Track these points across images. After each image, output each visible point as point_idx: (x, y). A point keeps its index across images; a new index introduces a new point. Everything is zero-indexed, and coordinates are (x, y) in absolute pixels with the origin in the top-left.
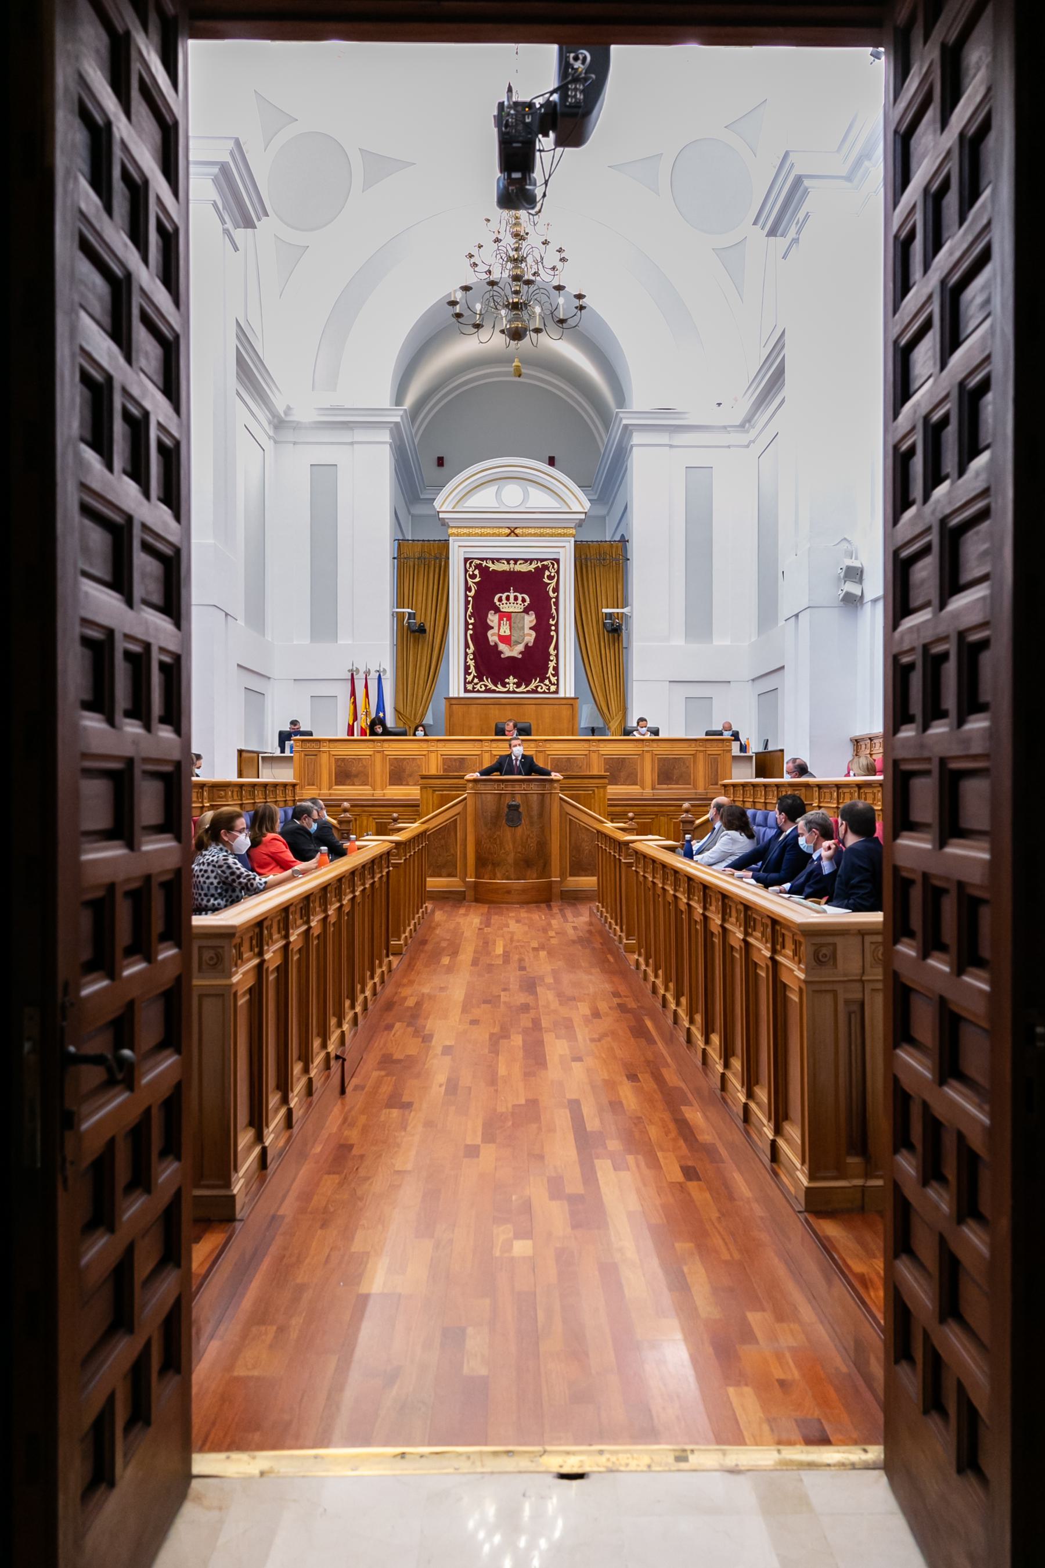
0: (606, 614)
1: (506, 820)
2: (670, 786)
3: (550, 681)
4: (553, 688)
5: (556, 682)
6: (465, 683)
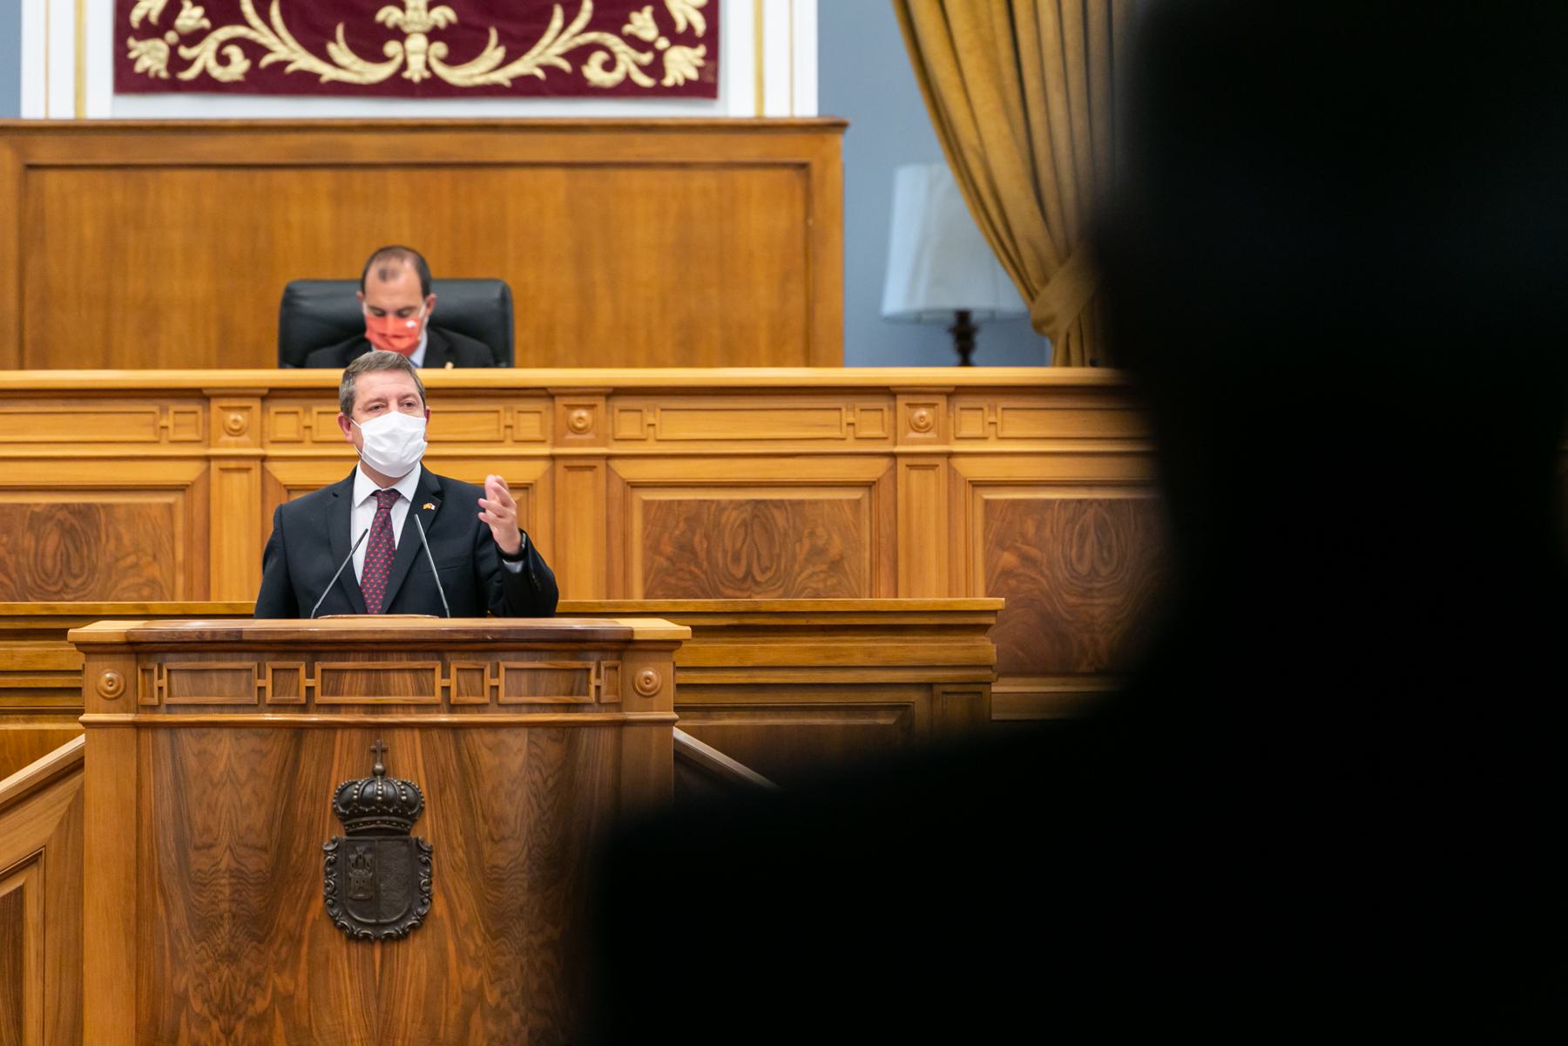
1: (336, 898)
4: (682, 64)
5: (700, 26)
6: (123, 31)
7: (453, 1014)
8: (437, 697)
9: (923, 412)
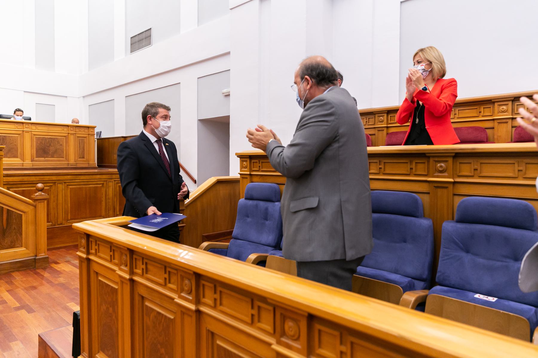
2: (46, 159)
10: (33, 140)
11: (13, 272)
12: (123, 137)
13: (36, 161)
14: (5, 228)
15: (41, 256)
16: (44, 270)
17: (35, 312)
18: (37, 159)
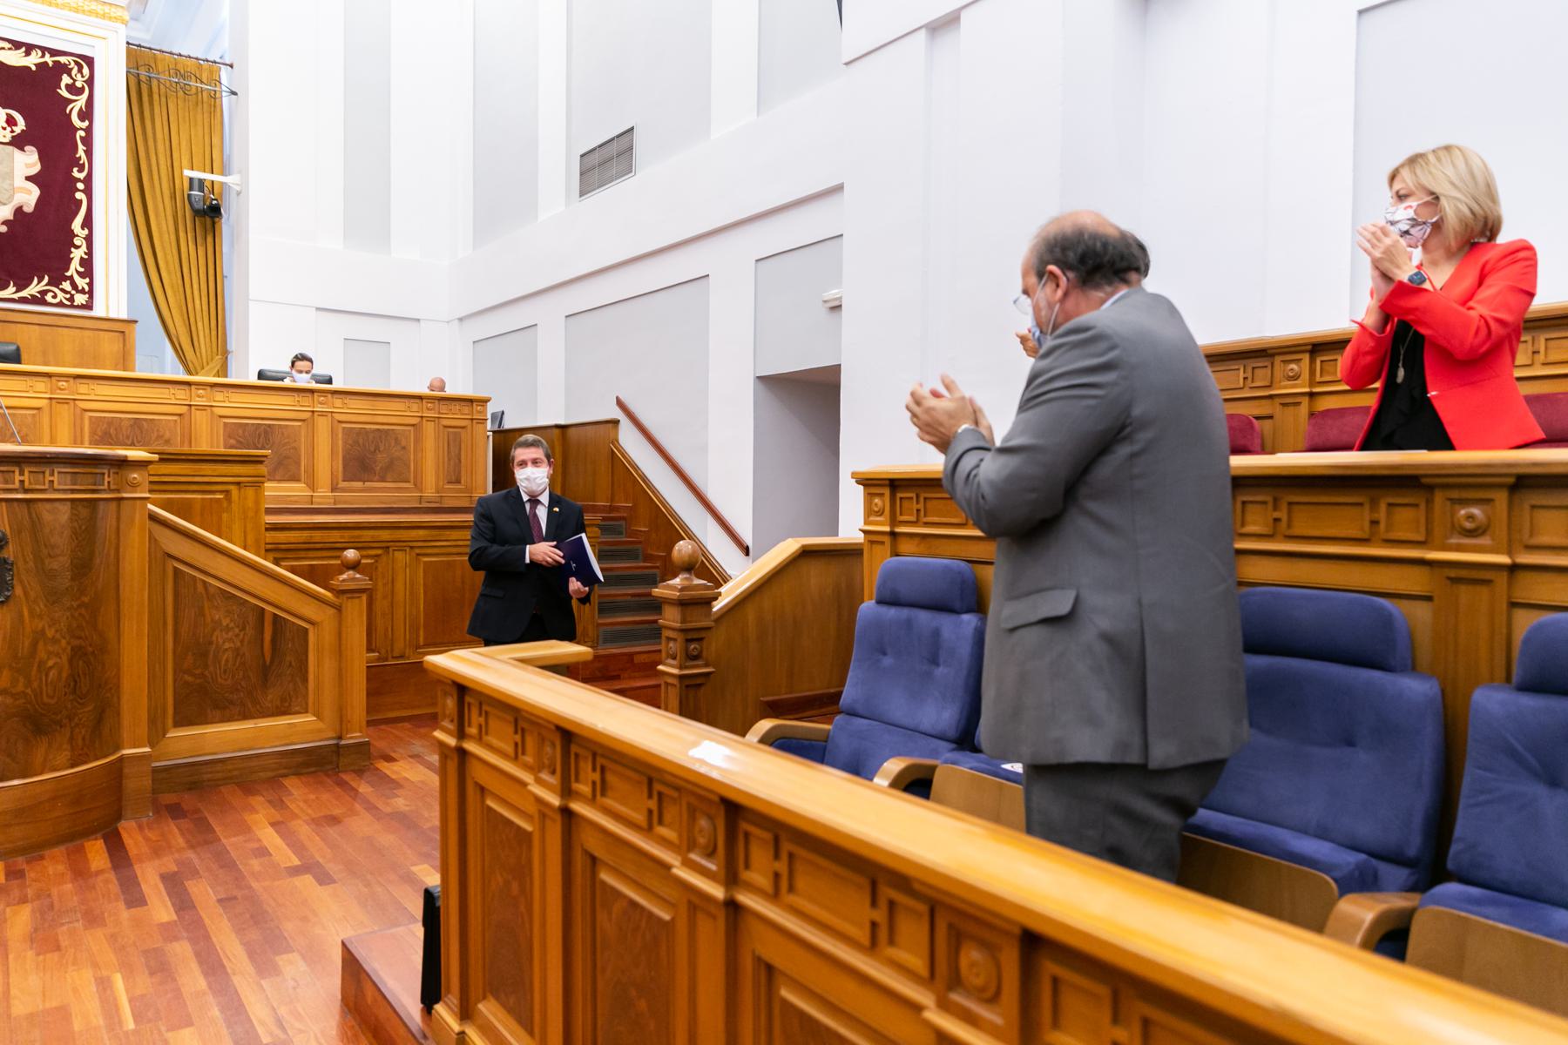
0: (191, 180)
2: (367, 484)
3: (74, 286)
4: (80, 299)
5: (87, 289)
7: (27, 643)
8: (17, 485)
9: (201, 391)
10: (337, 435)
11: (285, 776)
12: (557, 426)
13: (344, 490)
14: (268, 663)
15: (351, 738)
16: (358, 776)
17: (334, 882)
18: (346, 484)
